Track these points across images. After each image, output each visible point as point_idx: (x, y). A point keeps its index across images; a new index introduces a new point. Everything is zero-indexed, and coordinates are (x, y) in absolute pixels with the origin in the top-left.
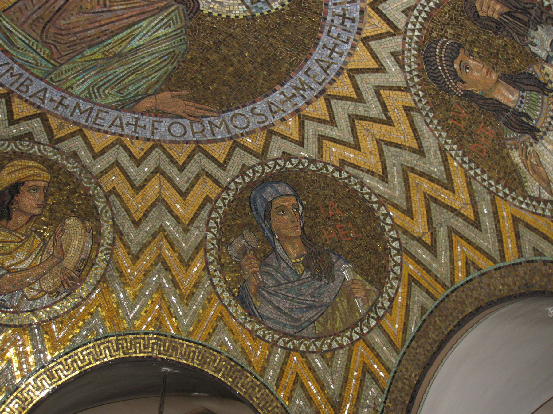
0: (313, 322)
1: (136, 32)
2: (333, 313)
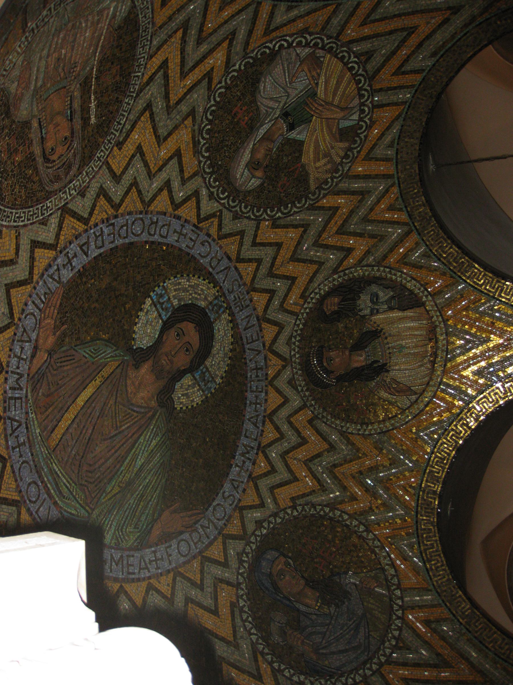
1: (138, 451)
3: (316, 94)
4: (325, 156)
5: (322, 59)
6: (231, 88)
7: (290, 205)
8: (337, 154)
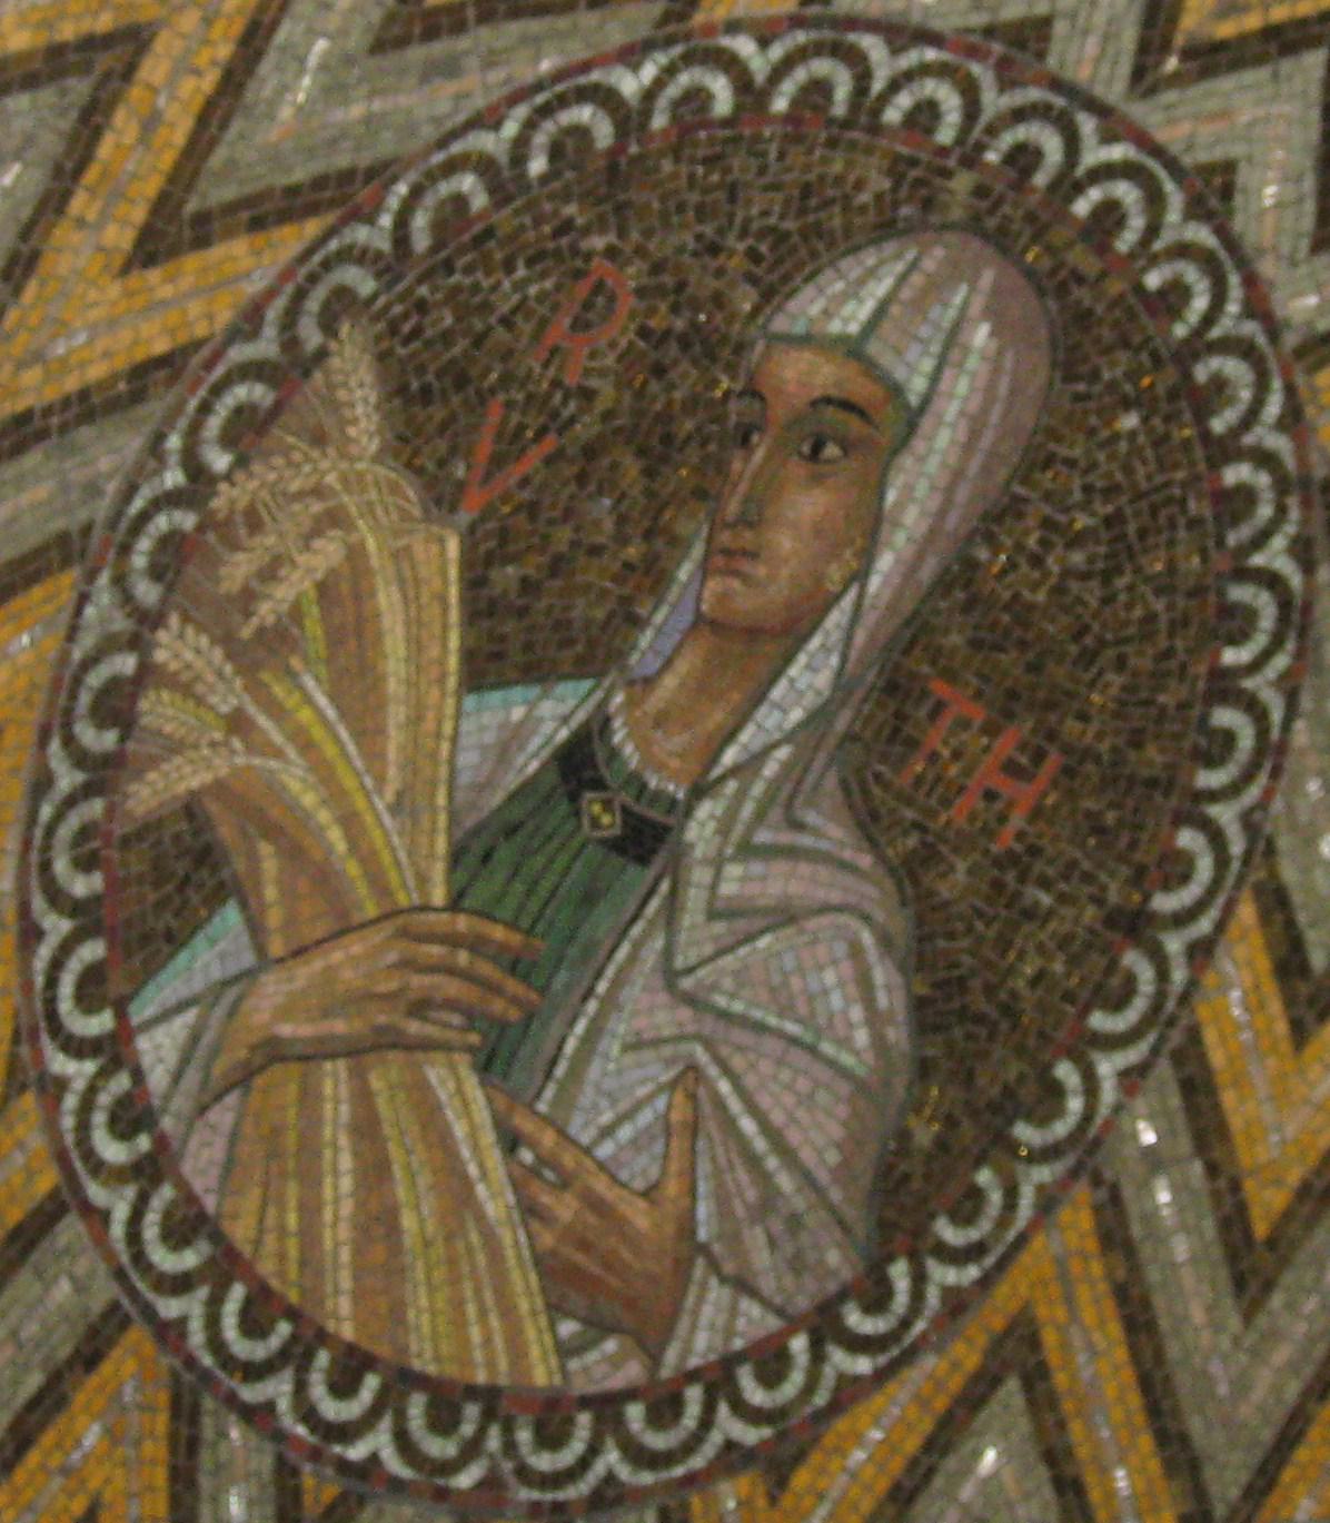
3: (486, 1065)
4: (280, 639)
5: (568, 1328)
6: (1111, 921)
7: (537, 165)
8: (185, 688)
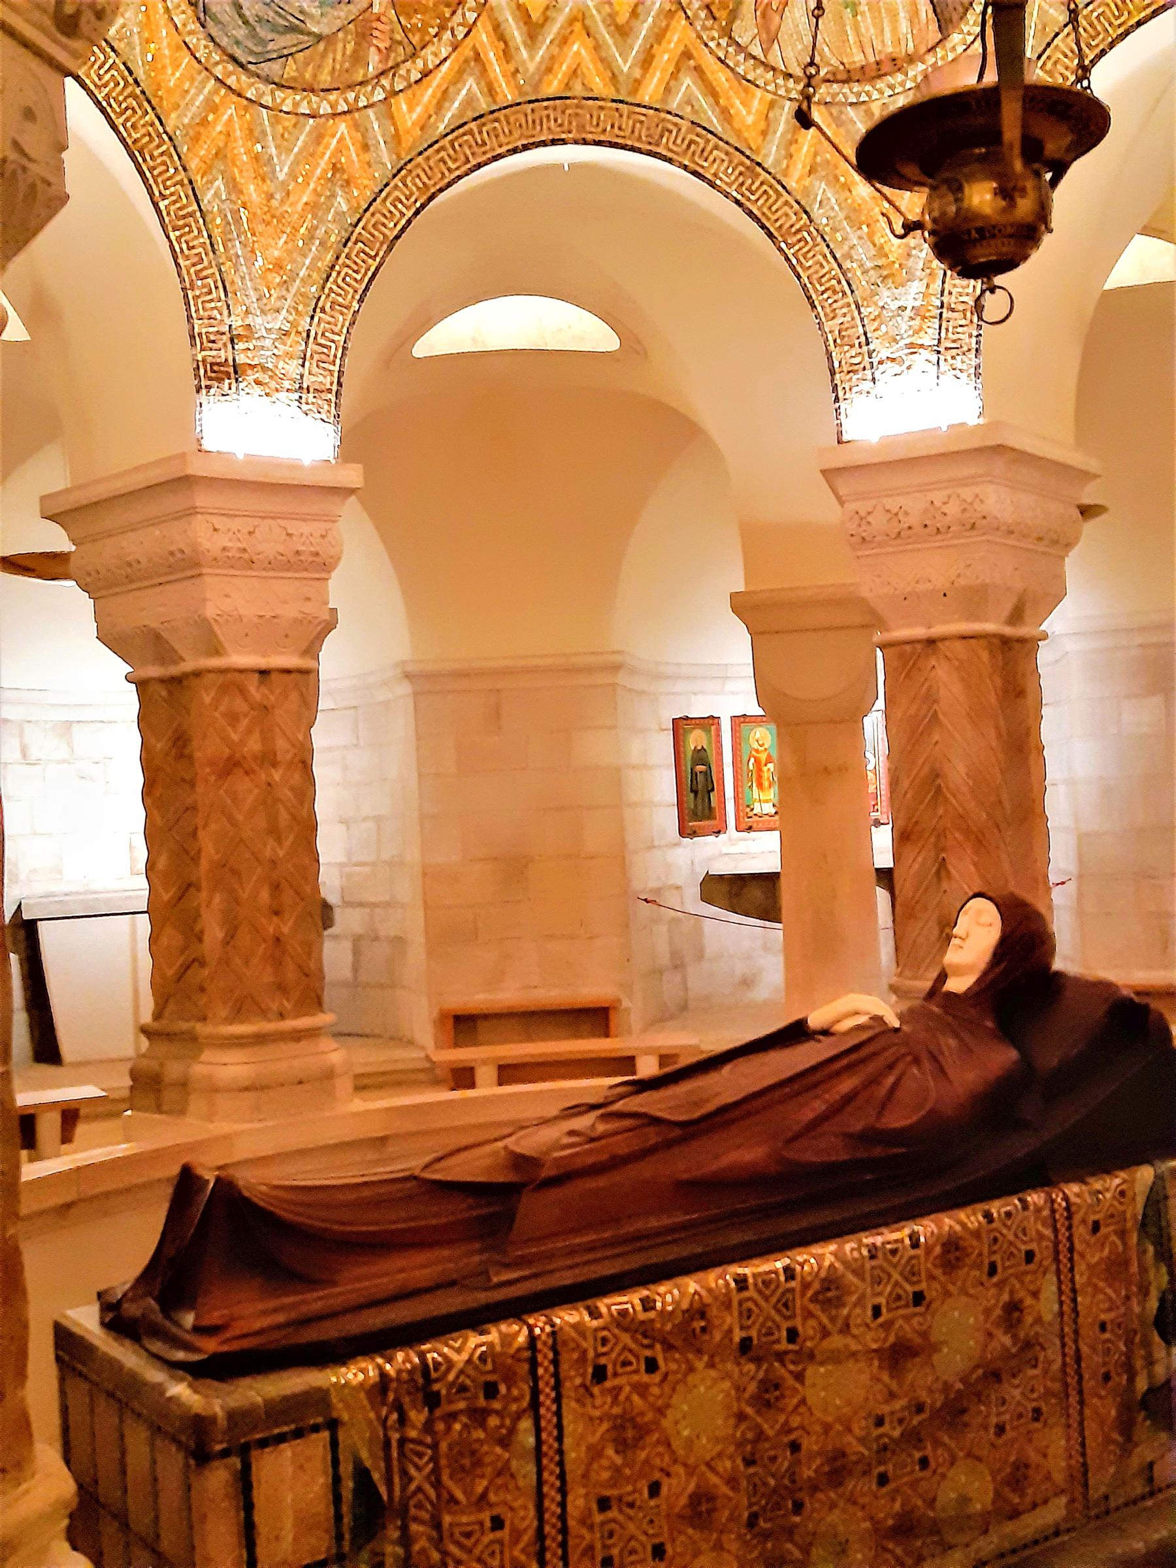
0: (286, 56)
2: (324, 55)
